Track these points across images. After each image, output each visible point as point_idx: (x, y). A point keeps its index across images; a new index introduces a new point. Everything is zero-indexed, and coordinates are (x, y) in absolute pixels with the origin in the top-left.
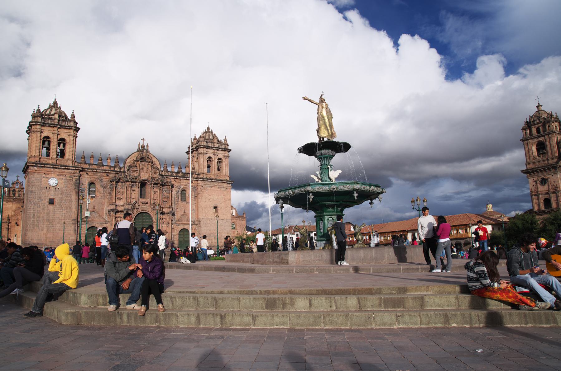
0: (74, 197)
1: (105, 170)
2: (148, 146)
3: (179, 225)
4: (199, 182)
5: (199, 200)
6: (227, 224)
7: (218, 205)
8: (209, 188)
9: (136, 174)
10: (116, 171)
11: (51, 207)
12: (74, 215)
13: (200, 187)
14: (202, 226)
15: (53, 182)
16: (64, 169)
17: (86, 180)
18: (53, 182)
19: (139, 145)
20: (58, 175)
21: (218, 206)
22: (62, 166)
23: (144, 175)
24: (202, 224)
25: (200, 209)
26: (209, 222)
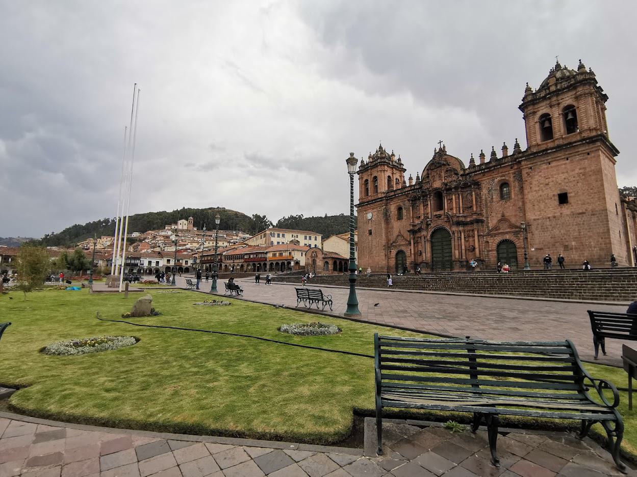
0: (383, 225)
1: (405, 192)
2: (444, 147)
3: (495, 235)
4: (523, 163)
5: (526, 192)
6: (594, 219)
7: (567, 188)
8: (544, 166)
9: (428, 186)
10: (417, 189)
11: (370, 237)
12: (384, 242)
13: (524, 172)
14: (536, 233)
15: (369, 216)
16: (375, 202)
17: (393, 208)
18: (369, 216)
19: (435, 150)
20: (373, 209)
21: (568, 191)
22: (372, 201)
23: (437, 184)
24: (533, 228)
25: (528, 206)
26: (548, 223)
